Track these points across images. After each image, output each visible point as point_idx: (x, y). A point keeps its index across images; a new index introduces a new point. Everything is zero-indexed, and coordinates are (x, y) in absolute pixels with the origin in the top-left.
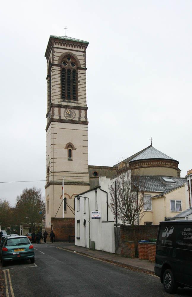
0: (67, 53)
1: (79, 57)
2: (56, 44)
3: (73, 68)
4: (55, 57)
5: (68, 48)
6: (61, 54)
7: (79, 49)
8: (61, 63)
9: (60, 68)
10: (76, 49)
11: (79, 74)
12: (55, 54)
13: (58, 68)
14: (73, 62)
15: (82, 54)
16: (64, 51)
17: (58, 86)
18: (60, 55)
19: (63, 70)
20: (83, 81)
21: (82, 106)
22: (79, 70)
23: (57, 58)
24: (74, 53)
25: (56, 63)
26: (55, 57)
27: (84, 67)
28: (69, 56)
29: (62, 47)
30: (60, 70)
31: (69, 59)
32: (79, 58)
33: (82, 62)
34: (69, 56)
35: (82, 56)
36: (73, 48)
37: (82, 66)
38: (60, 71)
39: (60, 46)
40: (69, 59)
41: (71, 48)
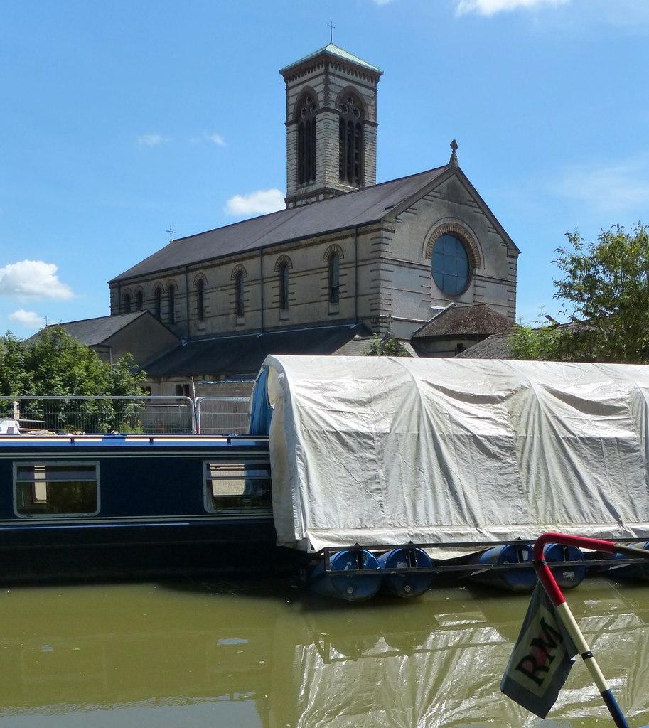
9: (295, 125)
11: (317, 124)
12: (290, 103)
13: (293, 127)
15: (321, 79)
16: (299, 89)
21: (319, 186)
23: (291, 110)
24: (311, 84)
33: (321, 97)
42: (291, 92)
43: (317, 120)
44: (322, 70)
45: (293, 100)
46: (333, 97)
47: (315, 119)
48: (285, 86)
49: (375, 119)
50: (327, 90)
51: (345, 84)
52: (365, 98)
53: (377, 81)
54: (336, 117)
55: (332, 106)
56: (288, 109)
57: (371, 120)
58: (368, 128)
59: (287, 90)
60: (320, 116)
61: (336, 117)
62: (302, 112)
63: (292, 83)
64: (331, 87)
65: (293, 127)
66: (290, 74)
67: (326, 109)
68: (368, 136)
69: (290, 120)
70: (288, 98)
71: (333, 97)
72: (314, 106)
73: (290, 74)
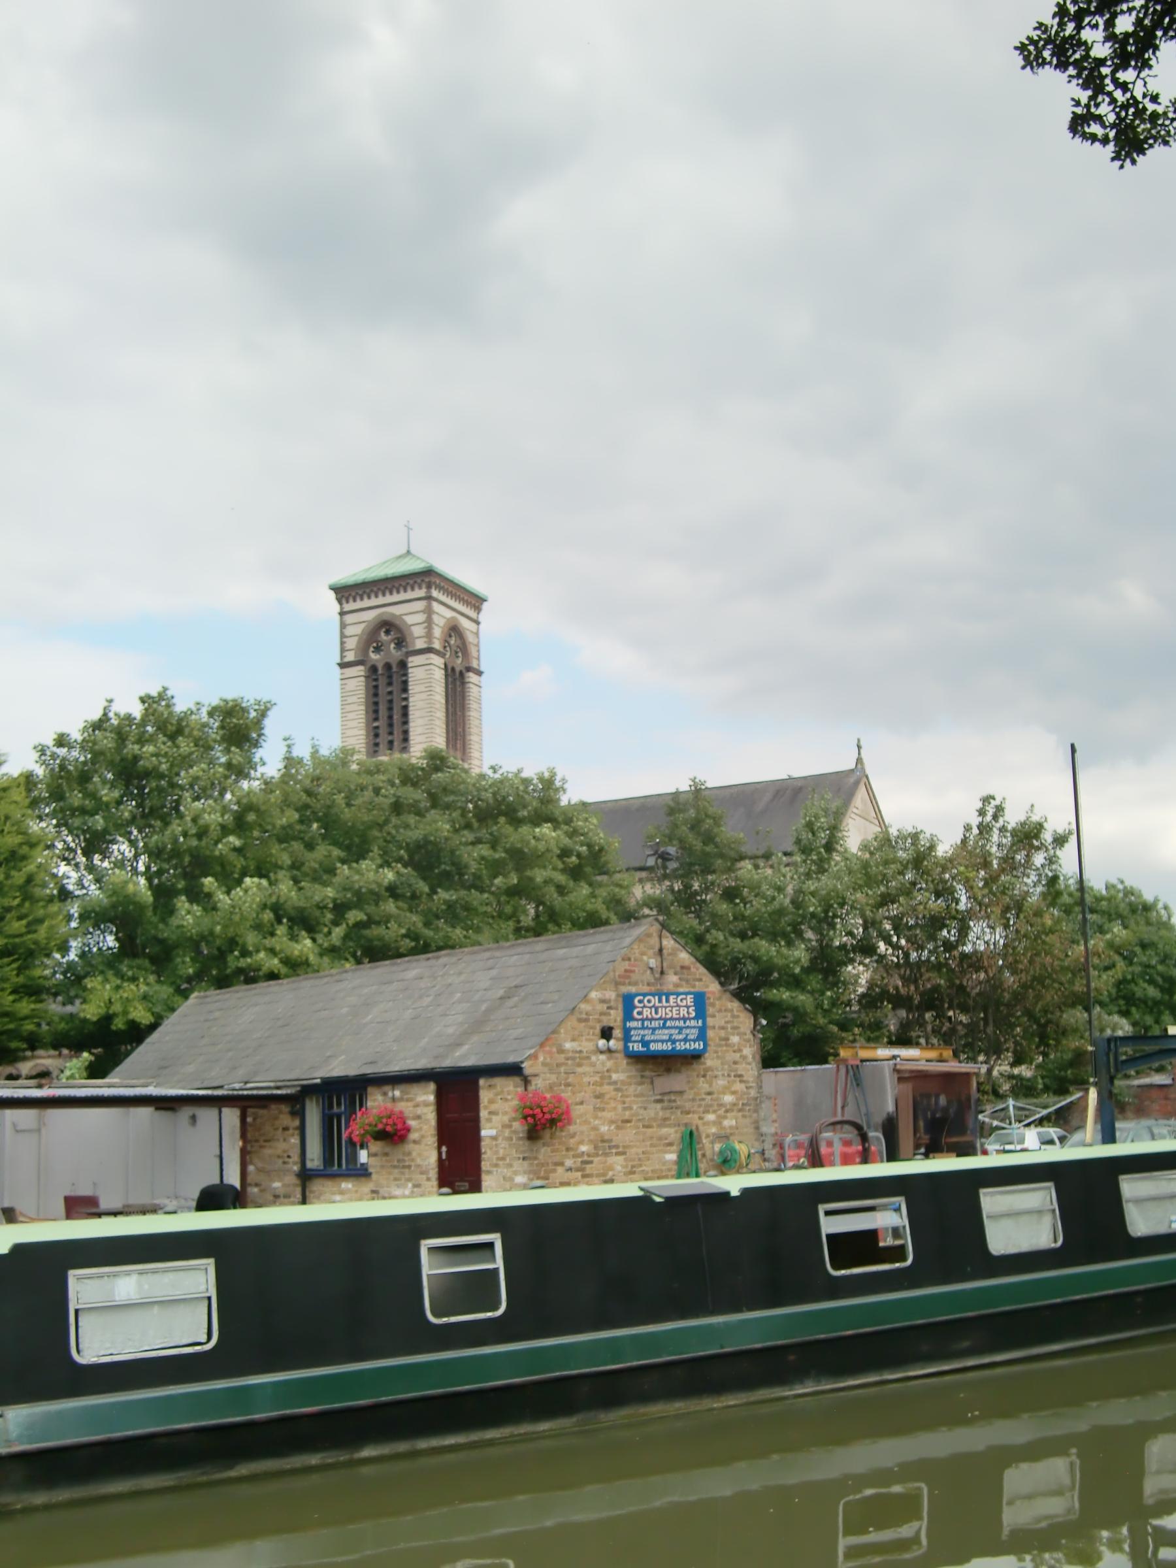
0: (379, 615)
1: (409, 620)
2: (347, 602)
4: (345, 640)
5: (381, 600)
6: (363, 625)
7: (410, 595)
9: (361, 668)
10: (402, 596)
11: (410, 670)
13: (359, 670)
14: (398, 639)
15: (421, 605)
16: (370, 616)
17: (354, 724)
19: (373, 669)
20: (422, 688)
22: (410, 659)
23: (352, 643)
24: (396, 610)
25: (350, 657)
26: (345, 640)
27: (424, 646)
28: (388, 625)
29: (366, 603)
30: (363, 673)
33: (418, 631)
34: (388, 625)
36: (396, 597)
37: (420, 644)
38: (363, 679)
39: (359, 604)
40: (387, 632)
41: (389, 599)
42: (349, 619)
43: (410, 665)
44: (421, 593)
45: (355, 630)
46: (437, 632)
47: (403, 665)
48: (336, 607)
49: (479, 665)
50: (429, 623)
51: (449, 614)
52: (468, 632)
53: (478, 609)
54: (439, 661)
55: (437, 645)
56: (342, 643)
57: (474, 664)
58: (472, 677)
61: (439, 661)
62: (372, 649)
63: (348, 607)
64: (435, 618)
65: (359, 670)
66: (344, 592)
67: (429, 650)
68: (473, 691)
69: (346, 660)
70: (343, 626)
71: (437, 632)
72: (400, 642)
73: (344, 592)
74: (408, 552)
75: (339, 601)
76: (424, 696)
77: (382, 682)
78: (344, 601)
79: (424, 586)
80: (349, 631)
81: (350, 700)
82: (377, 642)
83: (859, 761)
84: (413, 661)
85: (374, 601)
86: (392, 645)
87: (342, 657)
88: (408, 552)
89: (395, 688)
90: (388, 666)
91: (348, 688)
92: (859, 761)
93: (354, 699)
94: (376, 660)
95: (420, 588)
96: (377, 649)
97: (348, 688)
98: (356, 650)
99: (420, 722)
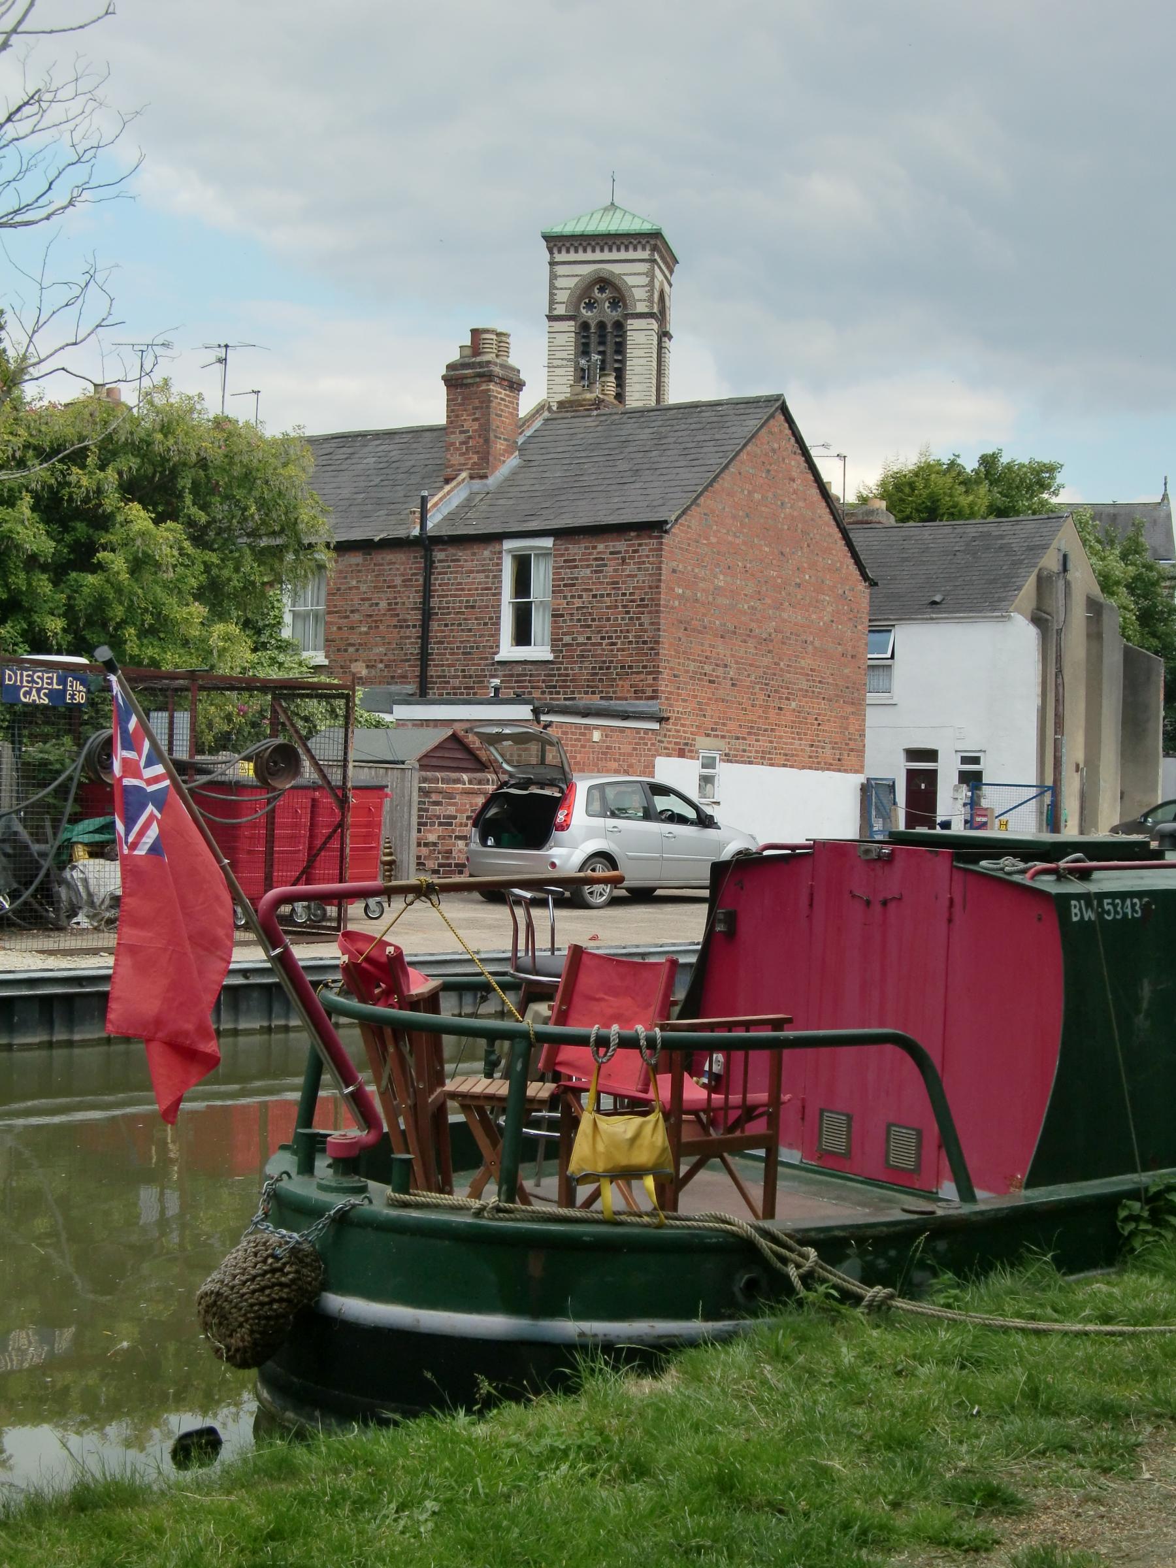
1: (631, 281)
2: (560, 252)
3: (611, 315)
5: (598, 256)
6: (577, 279)
7: (631, 255)
8: (577, 308)
9: (572, 323)
10: (623, 255)
11: (629, 333)
13: (569, 326)
14: (614, 298)
15: (643, 267)
17: (564, 380)
18: (571, 283)
19: (585, 326)
20: (641, 353)
22: (629, 321)
23: (562, 296)
24: (617, 269)
25: (561, 310)
27: (646, 310)
29: (581, 256)
30: (573, 329)
31: (602, 290)
32: (630, 284)
33: (639, 294)
34: (603, 283)
35: (639, 274)
36: (615, 255)
37: (641, 308)
38: (573, 335)
39: (572, 256)
40: (602, 290)
41: (606, 255)
42: (560, 270)
43: (629, 327)
44: (645, 255)
47: (619, 326)
48: (547, 256)
56: (552, 295)
59: (552, 264)
60: (632, 324)
63: (559, 257)
65: (569, 326)
69: (556, 313)
70: (553, 277)
73: (555, 242)
74: (612, 204)
75: (551, 252)
76: (643, 361)
77: (594, 339)
78: (555, 251)
79: (648, 248)
80: (560, 283)
81: (559, 355)
82: (590, 298)
83: (1165, 497)
84: (632, 324)
85: (589, 256)
86: (607, 304)
87: (551, 309)
88: (612, 204)
89: (610, 349)
90: (601, 325)
91: (557, 342)
92: (1165, 497)
93: (564, 355)
94: (589, 317)
95: (644, 249)
96: (590, 306)
97: (557, 342)
98: (567, 304)
99: (638, 387)
